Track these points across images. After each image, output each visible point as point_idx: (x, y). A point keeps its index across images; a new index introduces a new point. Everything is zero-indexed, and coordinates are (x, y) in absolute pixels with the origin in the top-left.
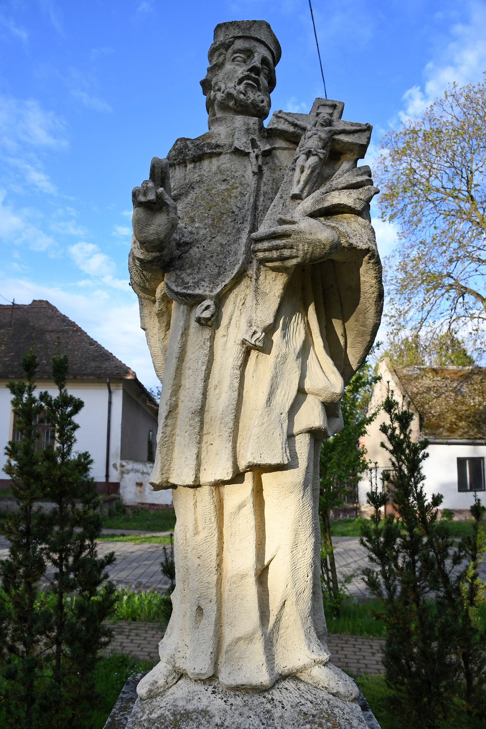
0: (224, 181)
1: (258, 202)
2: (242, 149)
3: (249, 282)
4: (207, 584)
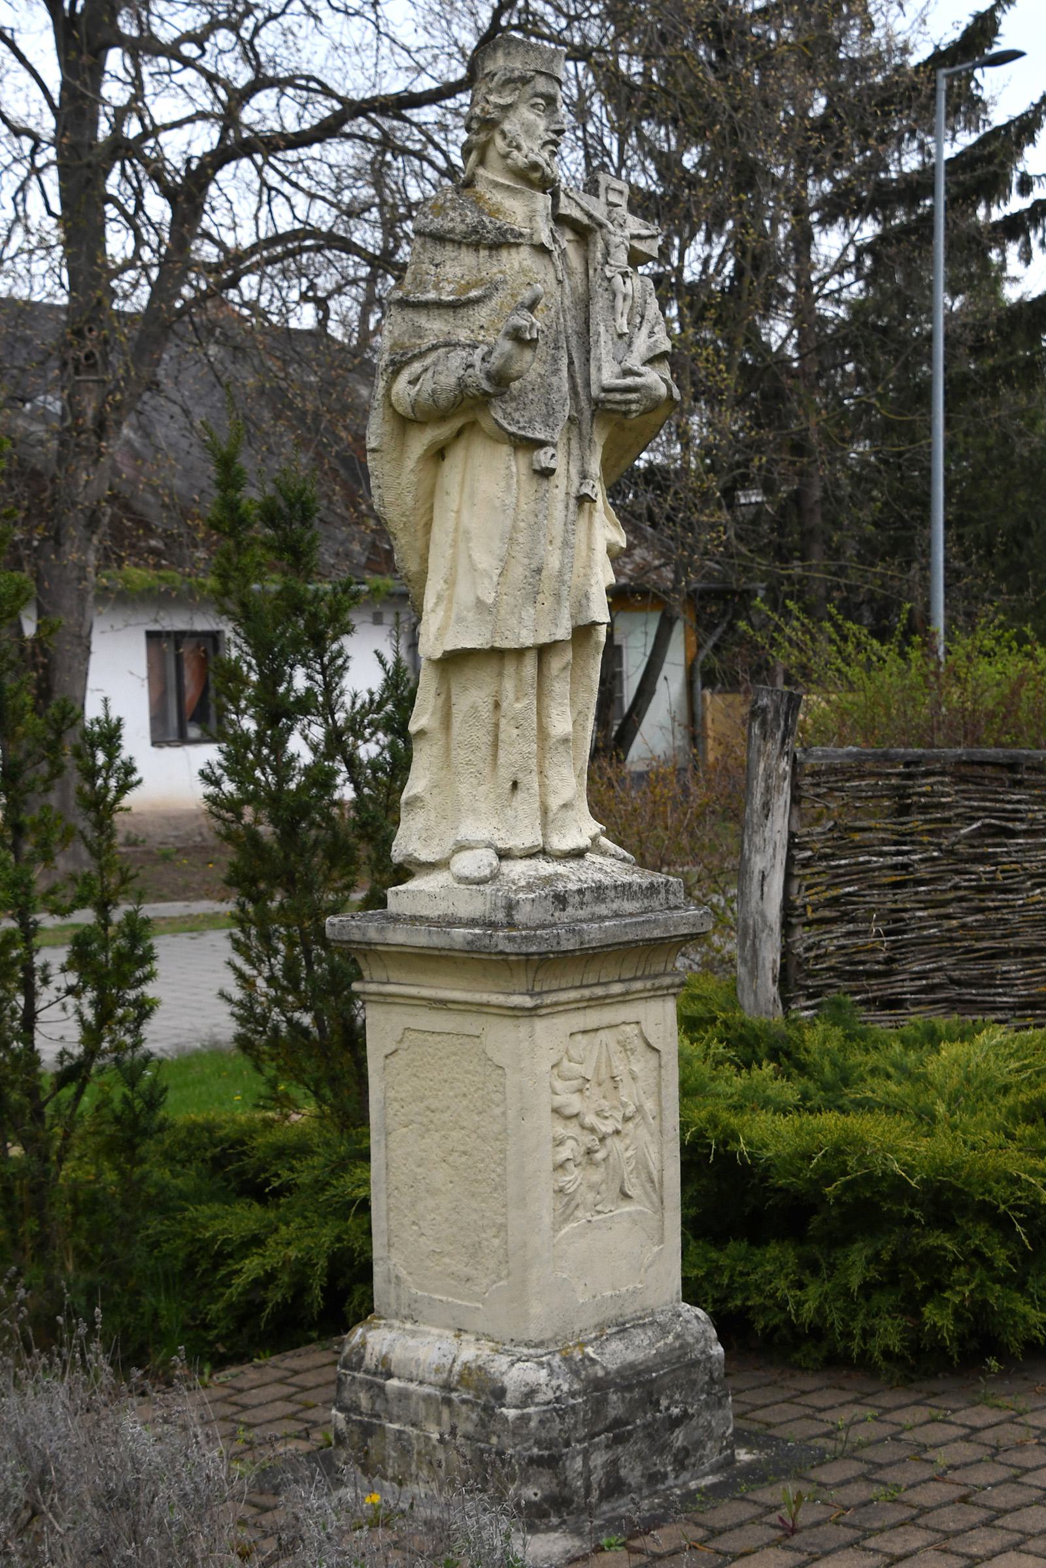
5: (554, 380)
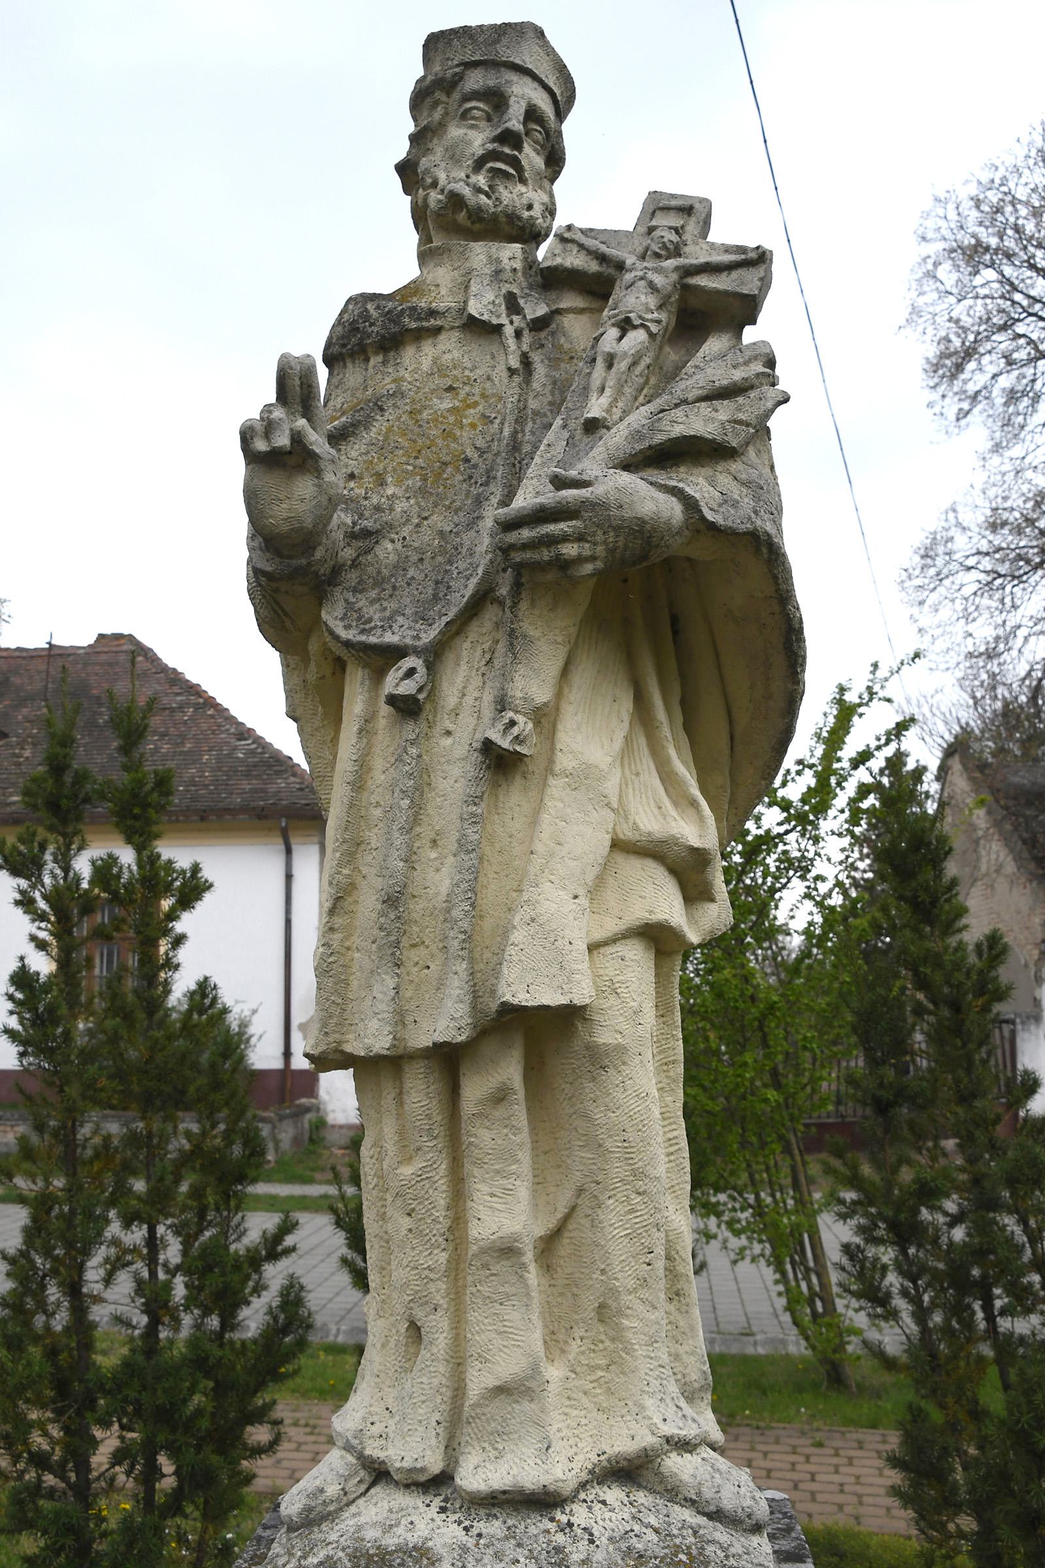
0: (450, 389)
1: (520, 435)
2: (485, 317)
3: (501, 613)
4: (426, 1272)
5: (467, 538)
